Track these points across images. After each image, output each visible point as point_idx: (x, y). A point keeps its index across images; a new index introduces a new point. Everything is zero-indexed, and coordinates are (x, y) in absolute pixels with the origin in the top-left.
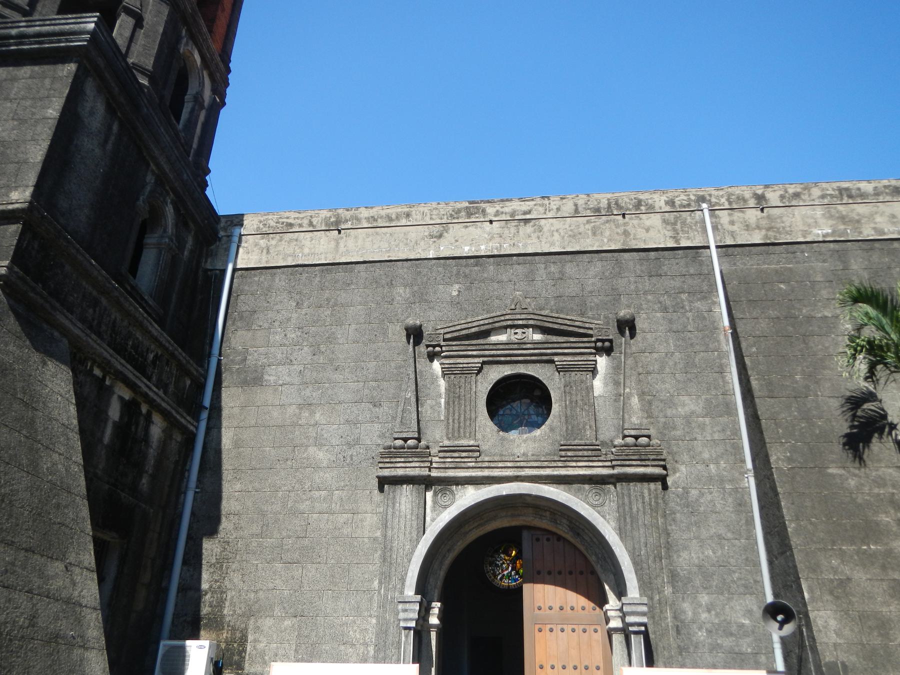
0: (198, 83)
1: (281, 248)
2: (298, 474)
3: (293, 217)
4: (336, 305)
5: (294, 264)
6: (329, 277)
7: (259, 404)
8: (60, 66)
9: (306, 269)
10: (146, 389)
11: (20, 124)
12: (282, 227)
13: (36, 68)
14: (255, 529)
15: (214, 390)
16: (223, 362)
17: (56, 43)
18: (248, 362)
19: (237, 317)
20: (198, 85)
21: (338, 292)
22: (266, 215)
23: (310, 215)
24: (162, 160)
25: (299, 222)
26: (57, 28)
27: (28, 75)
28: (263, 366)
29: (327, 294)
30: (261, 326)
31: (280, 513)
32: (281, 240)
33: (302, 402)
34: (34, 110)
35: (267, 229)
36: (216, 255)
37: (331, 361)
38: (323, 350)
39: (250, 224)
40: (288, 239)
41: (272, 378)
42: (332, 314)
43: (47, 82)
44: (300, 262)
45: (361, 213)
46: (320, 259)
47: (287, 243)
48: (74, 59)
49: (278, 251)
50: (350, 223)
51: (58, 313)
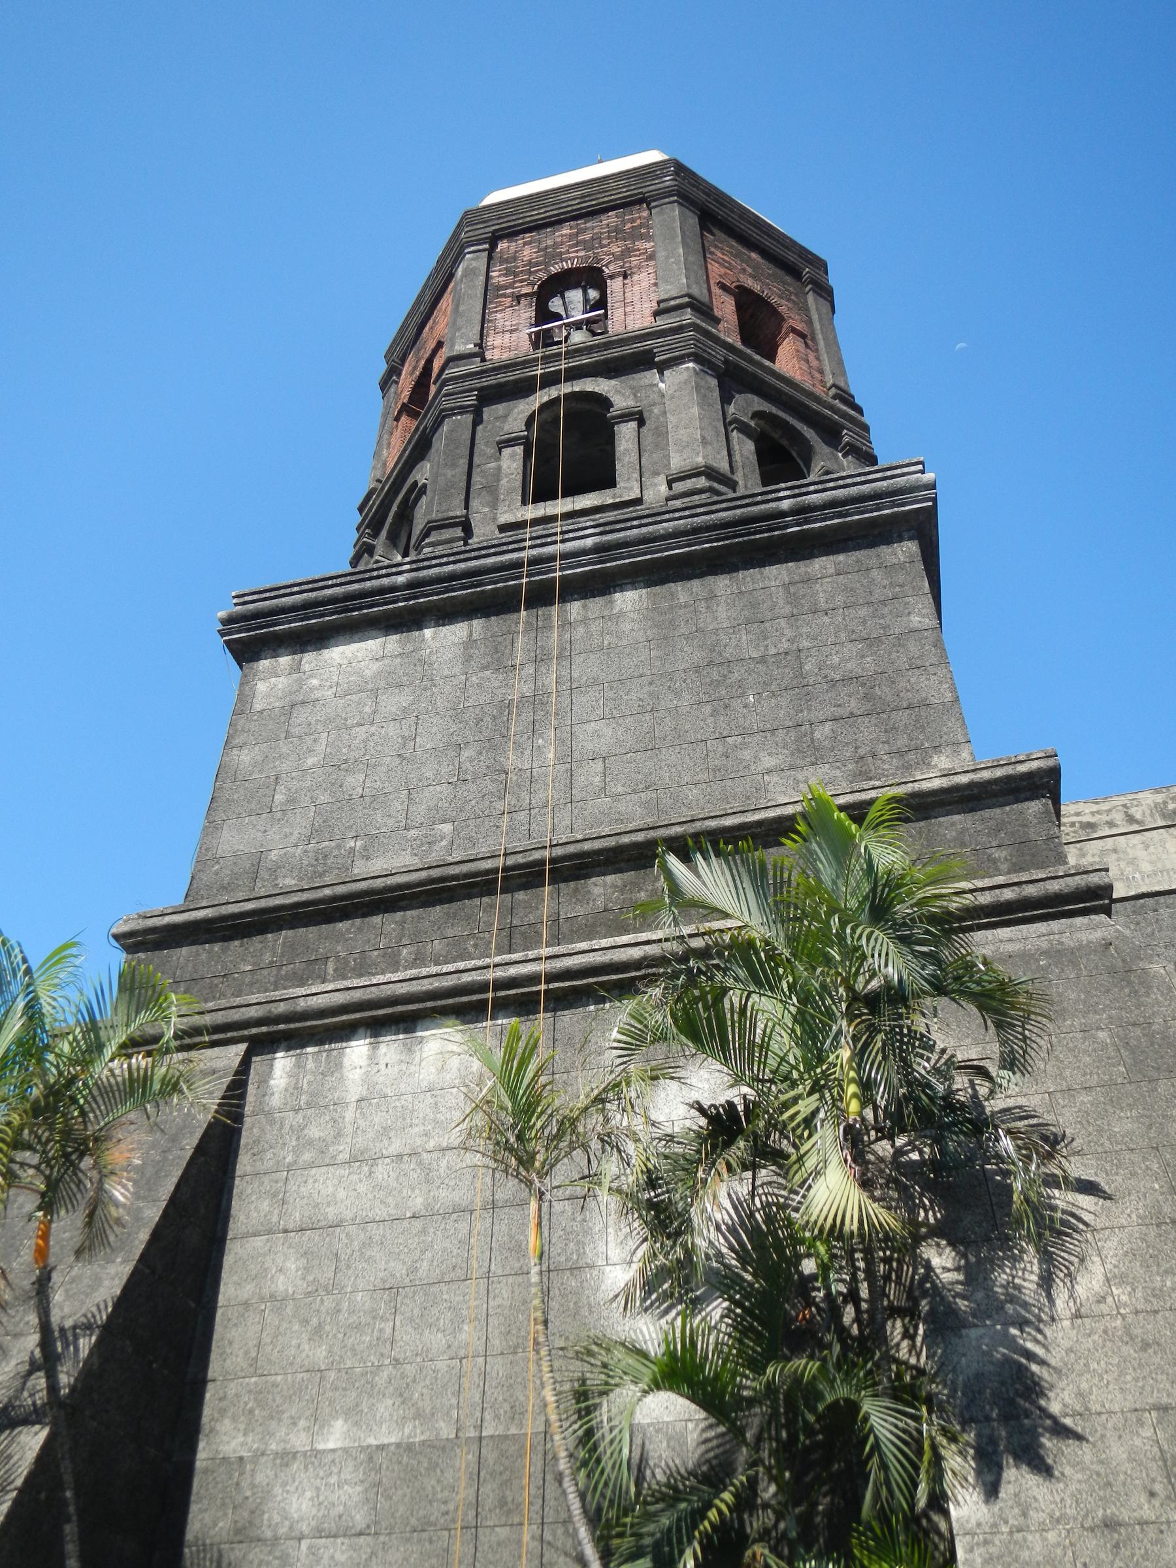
3: (1087, 811)
8: (884, 550)
9: (1162, 899)
11: (870, 646)
12: (1075, 832)
13: (841, 557)
23: (1121, 803)
25: (1105, 818)
27: (832, 571)
34: (882, 621)
43: (874, 573)
44: (1144, 889)
48: (906, 535)
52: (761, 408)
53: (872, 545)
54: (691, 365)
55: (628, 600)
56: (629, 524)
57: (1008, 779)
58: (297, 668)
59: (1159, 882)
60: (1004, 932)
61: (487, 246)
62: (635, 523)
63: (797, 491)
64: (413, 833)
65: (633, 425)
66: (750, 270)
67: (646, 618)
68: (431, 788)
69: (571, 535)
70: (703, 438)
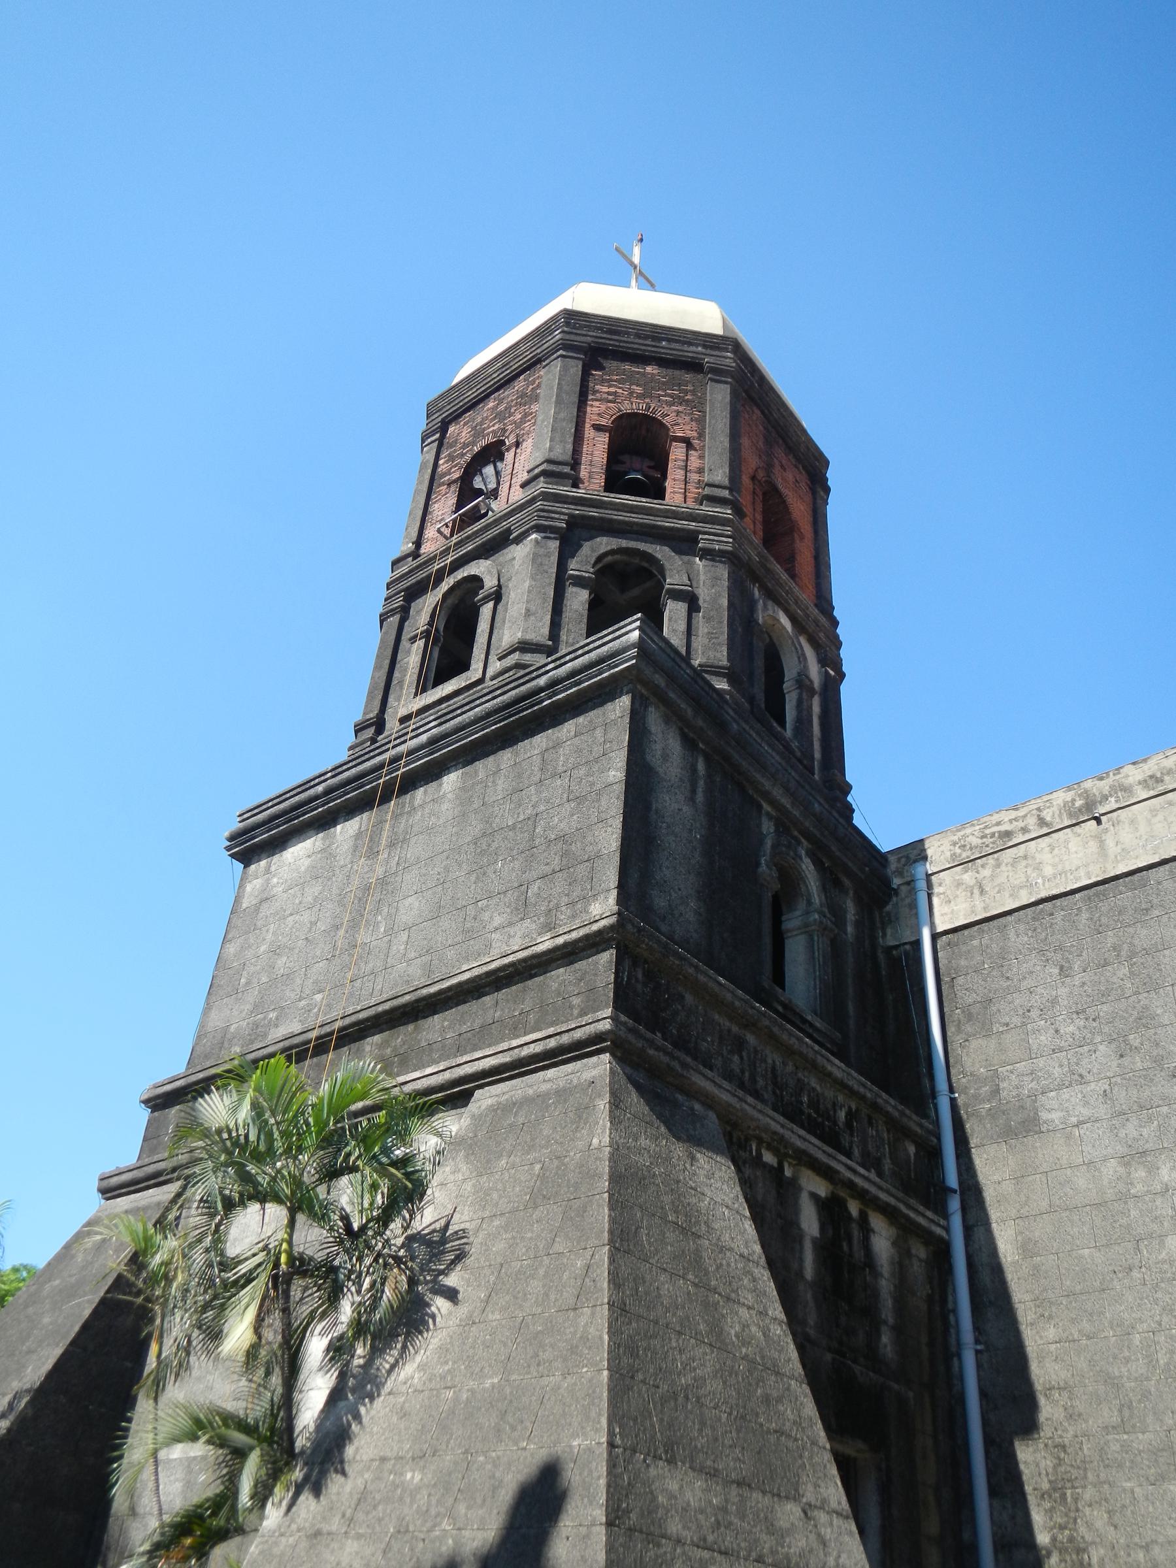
0: (796, 659)
1: (1002, 879)
2: (1159, 1295)
4: (1133, 954)
5: (1033, 900)
6: (1104, 907)
7: (1045, 1167)
8: (609, 706)
9: (1058, 902)
10: (849, 1174)
11: (579, 804)
13: (581, 719)
14: (1108, 1415)
15: (958, 1157)
16: (960, 1102)
17: (596, 676)
18: (1004, 1094)
19: (961, 1017)
20: (797, 662)
21: (1131, 930)
22: (959, 830)
23: (1035, 806)
24: (777, 793)
25: (1021, 824)
26: (593, 655)
27: (573, 733)
28: (1033, 1096)
29: (1110, 939)
30: (1007, 1025)
31: (1148, 1379)
32: (998, 866)
33: (1125, 1150)
35: (969, 853)
36: (897, 919)
37: (1159, 1061)
38: (1136, 1043)
39: (938, 852)
40: (1010, 860)
41: (1056, 1116)
42: (1131, 973)
43: (599, 733)
44: (1044, 894)
45: (1127, 776)
46: (1077, 879)
47: (1010, 868)
49: (999, 885)
50: (1113, 799)
51: (692, 1072)
52: (609, 548)
53: (602, 704)
54: (534, 536)
55: (451, 780)
56: (455, 714)
57: (587, 937)
58: (268, 870)
59: (1057, 886)
60: (551, 1073)
61: (438, 435)
62: (459, 712)
63: (558, 663)
64: (303, 1003)
65: (491, 604)
66: (639, 390)
67: (457, 798)
68: (317, 965)
69: (422, 730)
70: (528, 610)
